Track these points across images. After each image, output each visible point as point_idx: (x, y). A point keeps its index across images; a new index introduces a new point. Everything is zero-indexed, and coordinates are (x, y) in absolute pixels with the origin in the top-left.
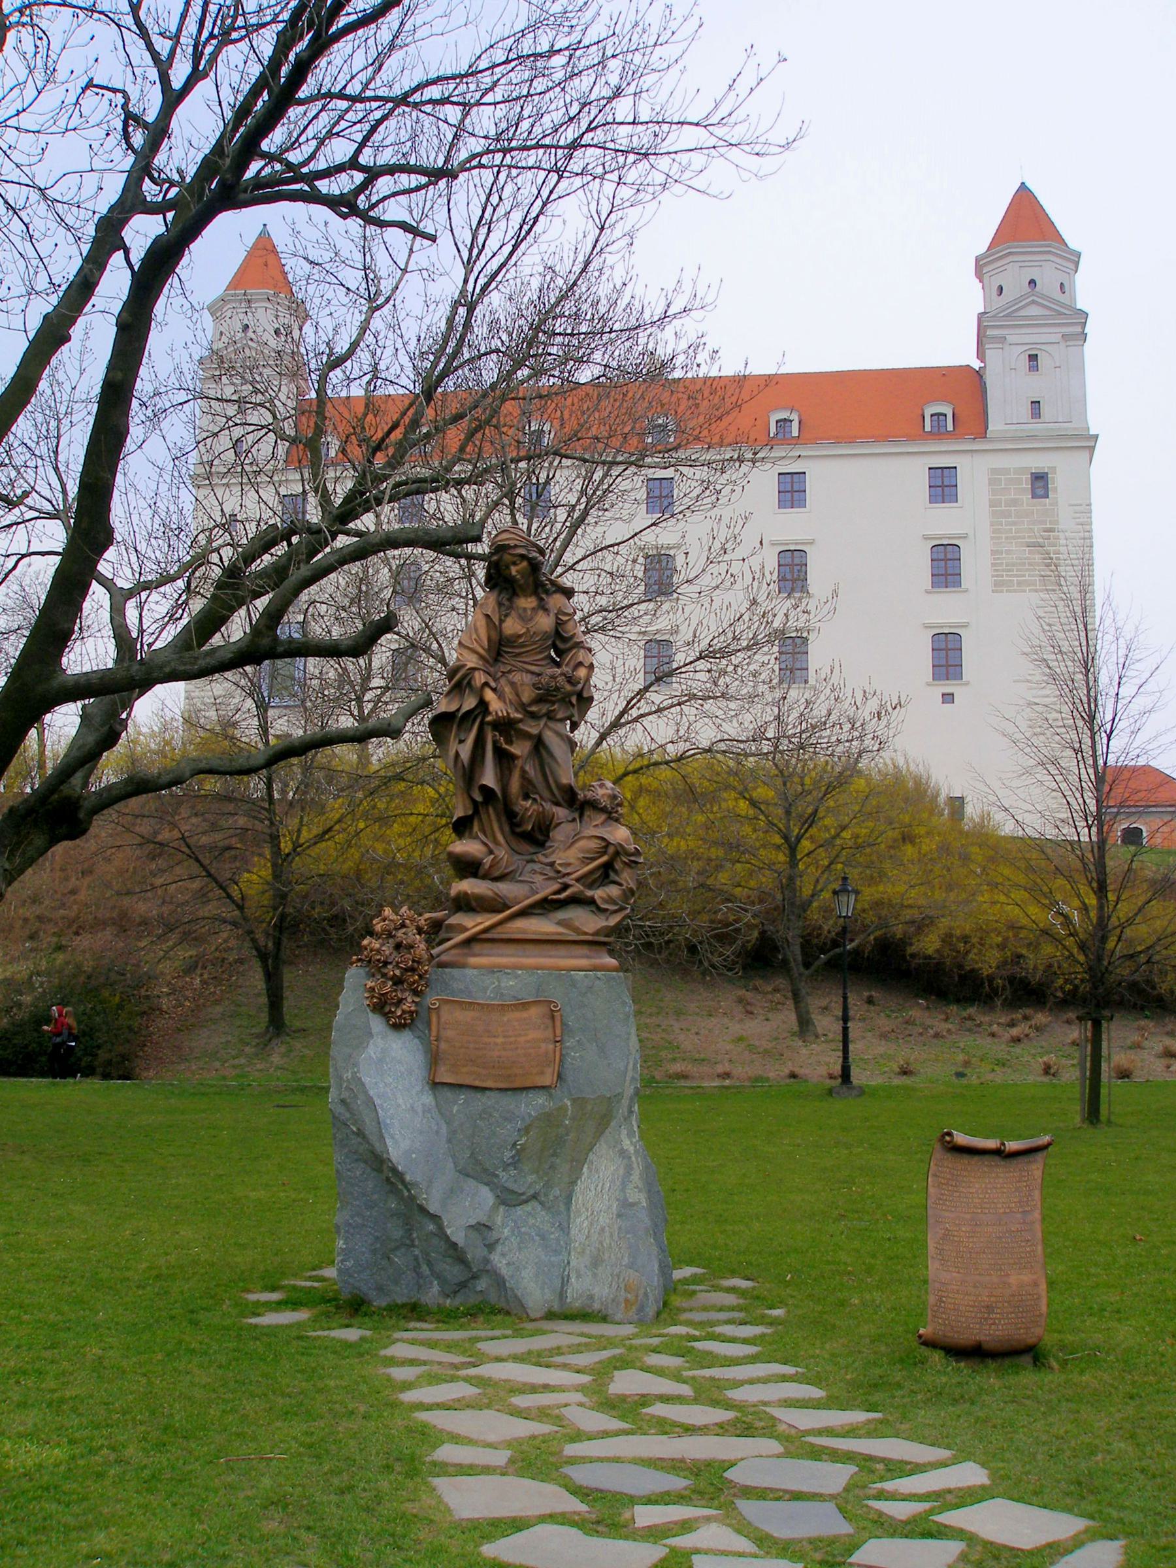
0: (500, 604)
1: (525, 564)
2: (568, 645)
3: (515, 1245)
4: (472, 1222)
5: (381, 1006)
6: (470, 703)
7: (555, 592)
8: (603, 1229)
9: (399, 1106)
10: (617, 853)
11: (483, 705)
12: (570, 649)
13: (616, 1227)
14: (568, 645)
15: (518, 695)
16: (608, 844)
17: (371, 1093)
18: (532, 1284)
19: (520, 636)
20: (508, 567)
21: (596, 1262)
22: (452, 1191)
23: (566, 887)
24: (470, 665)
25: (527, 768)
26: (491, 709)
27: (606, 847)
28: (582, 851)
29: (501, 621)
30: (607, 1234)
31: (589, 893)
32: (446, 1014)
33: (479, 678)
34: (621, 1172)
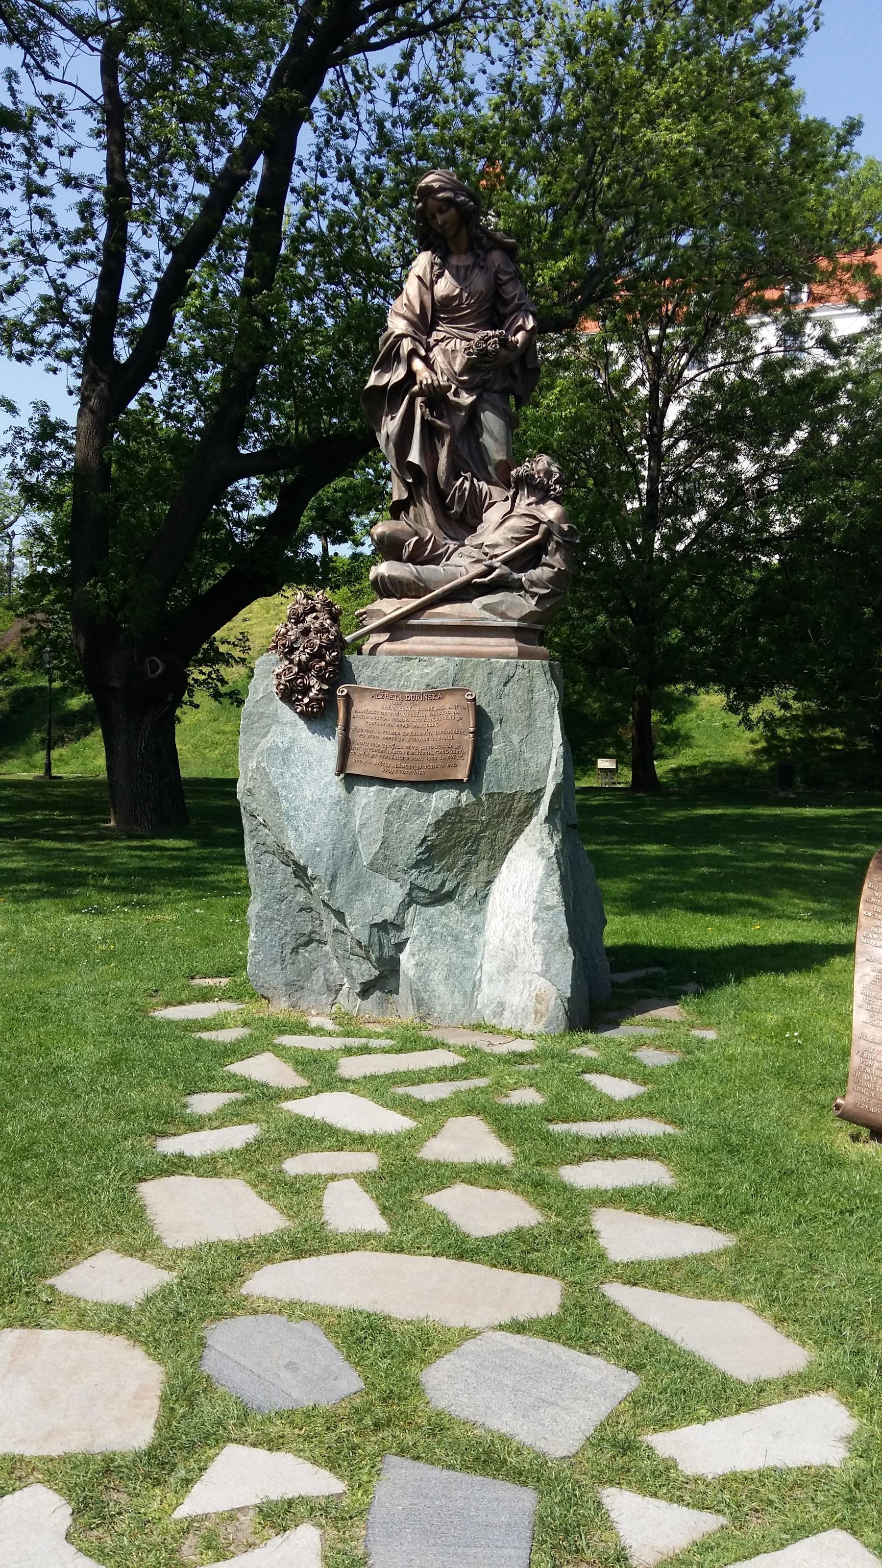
0: (432, 265)
1: (452, 211)
2: (510, 309)
3: (425, 945)
4: (378, 919)
5: (290, 694)
6: (400, 373)
7: (492, 249)
8: (518, 934)
9: (305, 797)
10: (548, 534)
11: (411, 375)
12: (511, 314)
13: (531, 931)
14: (510, 309)
15: (450, 364)
16: (541, 522)
17: (276, 783)
18: (442, 988)
19: (454, 298)
20: (434, 217)
21: (509, 968)
22: (358, 886)
23: (491, 569)
24: (398, 332)
25: (459, 445)
26: (418, 379)
27: (536, 527)
28: (512, 529)
29: (433, 283)
30: (522, 938)
31: (516, 576)
32: (361, 706)
33: (406, 345)
34: (540, 872)
